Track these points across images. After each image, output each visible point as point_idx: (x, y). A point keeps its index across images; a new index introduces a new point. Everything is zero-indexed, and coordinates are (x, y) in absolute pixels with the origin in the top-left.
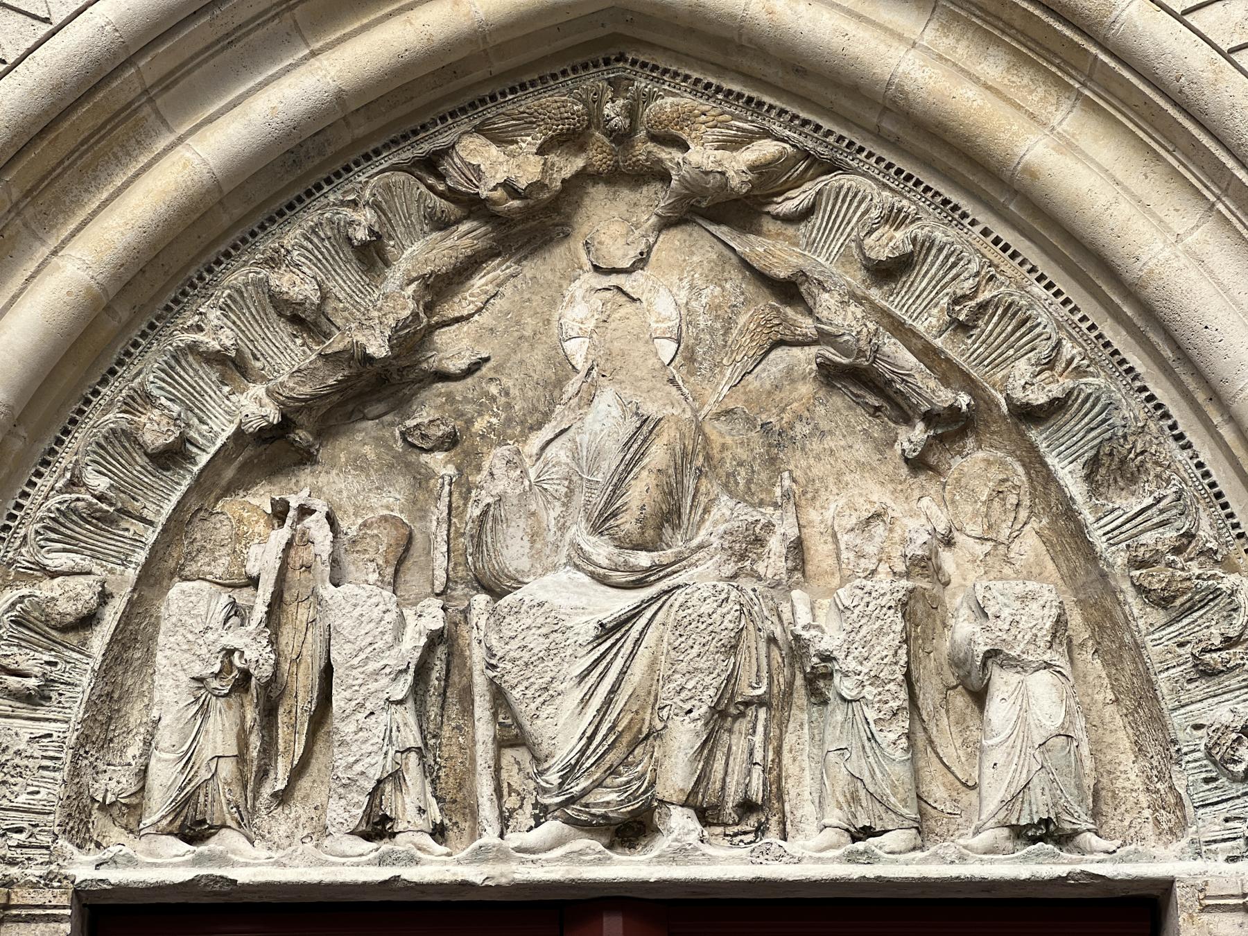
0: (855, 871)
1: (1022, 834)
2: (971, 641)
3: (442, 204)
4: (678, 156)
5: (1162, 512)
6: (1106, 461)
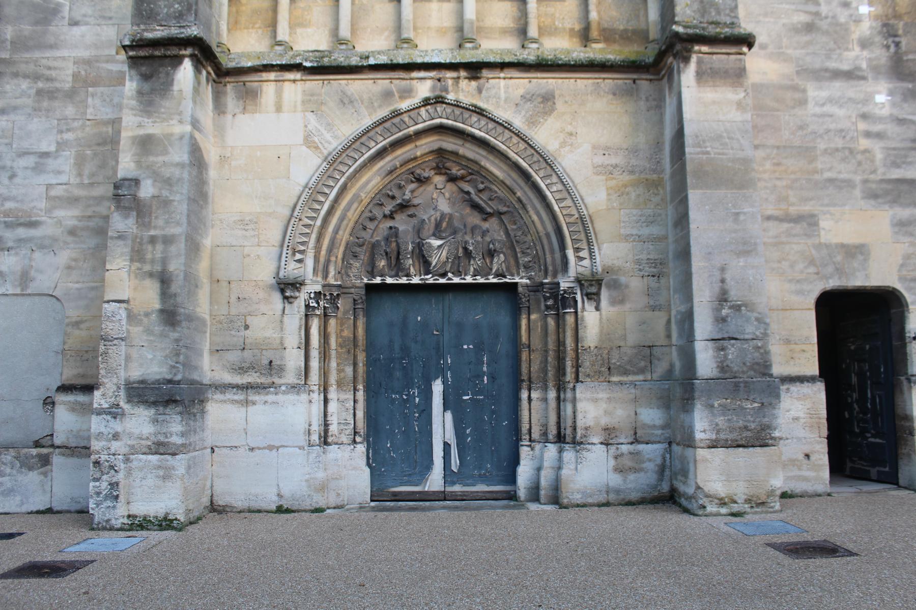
1: (499, 275)
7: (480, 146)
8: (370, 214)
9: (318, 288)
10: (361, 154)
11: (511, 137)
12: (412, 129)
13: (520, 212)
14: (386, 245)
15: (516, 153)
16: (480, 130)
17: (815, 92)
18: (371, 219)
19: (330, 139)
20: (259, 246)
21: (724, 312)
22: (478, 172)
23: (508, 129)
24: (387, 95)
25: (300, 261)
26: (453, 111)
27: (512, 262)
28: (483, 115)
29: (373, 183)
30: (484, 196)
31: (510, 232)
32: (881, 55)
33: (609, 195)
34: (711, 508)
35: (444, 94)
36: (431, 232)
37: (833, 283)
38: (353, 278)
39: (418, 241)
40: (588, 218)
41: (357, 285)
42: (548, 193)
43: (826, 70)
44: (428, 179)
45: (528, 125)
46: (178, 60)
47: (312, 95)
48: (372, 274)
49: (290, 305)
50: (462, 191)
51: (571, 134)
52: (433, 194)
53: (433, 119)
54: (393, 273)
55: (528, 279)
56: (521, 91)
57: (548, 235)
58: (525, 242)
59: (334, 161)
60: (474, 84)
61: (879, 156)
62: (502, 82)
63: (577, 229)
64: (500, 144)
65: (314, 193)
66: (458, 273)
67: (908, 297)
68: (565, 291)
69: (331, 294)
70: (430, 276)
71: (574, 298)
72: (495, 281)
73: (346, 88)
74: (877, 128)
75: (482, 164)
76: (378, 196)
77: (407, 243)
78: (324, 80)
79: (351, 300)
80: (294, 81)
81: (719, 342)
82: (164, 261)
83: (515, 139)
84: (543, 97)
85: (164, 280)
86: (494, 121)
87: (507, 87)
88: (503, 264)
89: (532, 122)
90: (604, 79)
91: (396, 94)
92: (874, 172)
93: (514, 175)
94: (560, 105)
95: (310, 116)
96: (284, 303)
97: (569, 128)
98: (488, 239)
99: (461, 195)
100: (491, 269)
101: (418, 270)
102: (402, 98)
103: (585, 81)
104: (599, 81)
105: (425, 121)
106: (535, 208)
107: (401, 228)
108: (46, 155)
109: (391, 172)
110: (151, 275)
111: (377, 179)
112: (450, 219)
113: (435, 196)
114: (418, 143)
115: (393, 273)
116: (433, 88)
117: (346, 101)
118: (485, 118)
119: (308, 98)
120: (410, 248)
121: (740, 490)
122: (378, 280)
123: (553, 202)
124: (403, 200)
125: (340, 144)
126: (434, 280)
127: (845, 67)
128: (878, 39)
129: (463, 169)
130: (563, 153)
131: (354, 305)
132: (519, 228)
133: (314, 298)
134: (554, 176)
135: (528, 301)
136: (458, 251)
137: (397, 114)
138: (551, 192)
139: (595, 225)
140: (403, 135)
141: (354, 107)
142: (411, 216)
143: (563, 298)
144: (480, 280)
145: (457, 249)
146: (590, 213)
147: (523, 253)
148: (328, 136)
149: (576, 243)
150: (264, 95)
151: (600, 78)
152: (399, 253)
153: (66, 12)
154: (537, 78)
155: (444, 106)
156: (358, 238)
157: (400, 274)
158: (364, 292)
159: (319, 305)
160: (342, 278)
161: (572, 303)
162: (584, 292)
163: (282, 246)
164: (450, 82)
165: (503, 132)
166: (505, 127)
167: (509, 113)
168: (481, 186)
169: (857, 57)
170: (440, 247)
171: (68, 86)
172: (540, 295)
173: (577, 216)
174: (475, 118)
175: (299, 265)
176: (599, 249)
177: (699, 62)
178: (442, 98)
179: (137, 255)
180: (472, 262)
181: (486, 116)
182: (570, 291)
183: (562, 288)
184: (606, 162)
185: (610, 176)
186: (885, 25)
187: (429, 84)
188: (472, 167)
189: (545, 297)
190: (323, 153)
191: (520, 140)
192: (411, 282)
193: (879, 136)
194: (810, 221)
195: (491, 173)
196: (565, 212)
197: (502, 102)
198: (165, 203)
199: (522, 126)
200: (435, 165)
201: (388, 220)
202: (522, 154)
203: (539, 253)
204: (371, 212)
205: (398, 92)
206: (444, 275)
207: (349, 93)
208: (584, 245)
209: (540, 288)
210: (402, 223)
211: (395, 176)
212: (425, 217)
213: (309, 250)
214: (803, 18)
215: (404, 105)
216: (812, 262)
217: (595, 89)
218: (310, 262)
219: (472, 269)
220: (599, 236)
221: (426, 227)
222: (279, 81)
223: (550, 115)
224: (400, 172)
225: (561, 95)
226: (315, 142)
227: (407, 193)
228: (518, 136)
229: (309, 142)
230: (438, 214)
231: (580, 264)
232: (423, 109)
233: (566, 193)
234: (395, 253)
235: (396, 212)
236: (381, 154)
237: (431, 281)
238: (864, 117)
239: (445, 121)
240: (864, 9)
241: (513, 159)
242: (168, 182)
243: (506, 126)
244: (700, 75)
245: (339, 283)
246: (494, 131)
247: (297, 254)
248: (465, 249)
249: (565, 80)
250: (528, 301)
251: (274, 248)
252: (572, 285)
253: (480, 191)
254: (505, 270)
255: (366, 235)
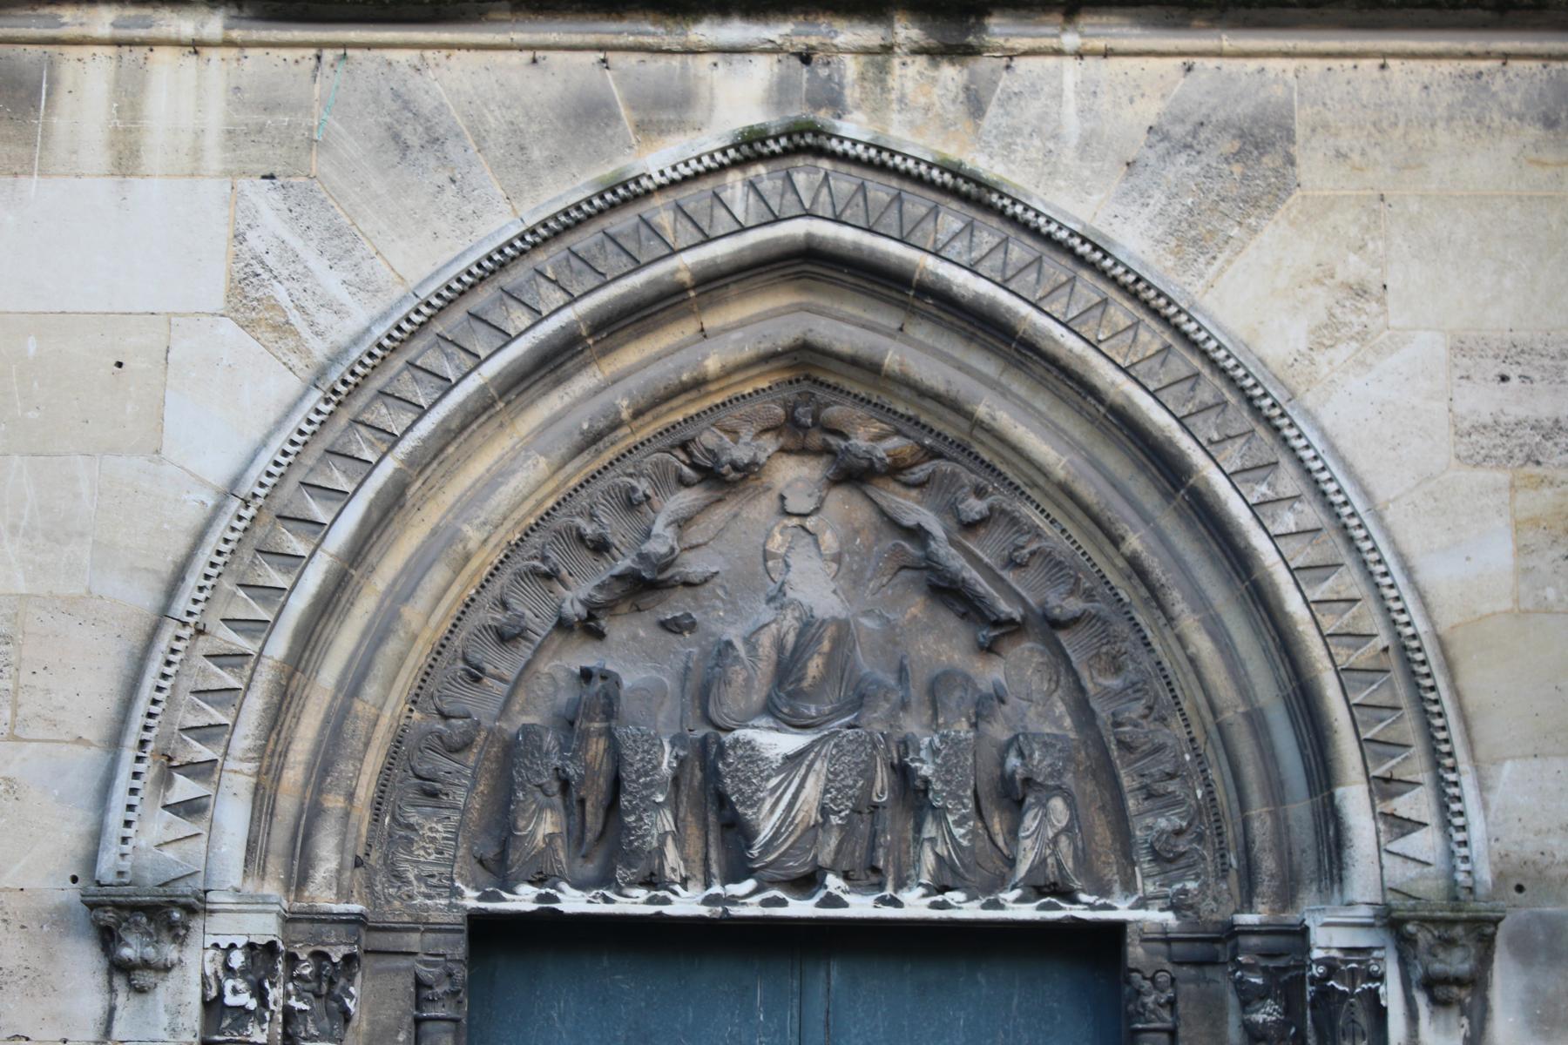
0: (936, 914)
1: (1038, 889)
2: (1014, 772)
3: (686, 470)
4: (843, 444)
5: (1135, 692)
6: (1104, 657)
7: (970, 339)
8: (500, 616)
9: (264, 928)
10: (469, 362)
11: (1105, 302)
12: (689, 259)
13: (1139, 618)
14: (563, 748)
15: (1125, 371)
16: (972, 269)
18: (506, 637)
19: (342, 294)
20: (17, 739)
22: (964, 448)
23: (1092, 266)
25: (191, 809)
26: (862, 188)
27: (1102, 833)
28: (989, 208)
29: (518, 482)
30: (988, 548)
31: (1095, 705)
33: (1522, 550)
35: (823, 117)
36: (757, 698)
38: (418, 888)
39: (699, 733)
40: (1431, 652)
41: (435, 917)
42: (1259, 541)
44: (749, 471)
45: (1177, 252)
47: (269, 108)
48: (500, 874)
49: (136, 1000)
50: (892, 523)
51: (1360, 291)
52: (769, 535)
53: (777, 220)
54: (590, 869)
55: (1173, 907)
56: (1150, 110)
57: (1256, 720)
58: (1159, 749)
60: (951, 74)
62: (1069, 63)
63: (1383, 698)
64: (1058, 331)
66: (867, 876)
68: (1331, 966)
69: (320, 957)
70: (749, 884)
71: (1374, 996)
72: (1028, 912)
73: (416, 81)
75: (982, 411)
76: (536, 539)
77: (654, 742)
78: (321, 45)
79: (405, 984)
80: (196, 46)
83: (1122, 311)
84: (1241, 135)
86: (1035, 233)
87: (1090, 91)
88: (1064, 842)
90: (1506, 57)
91: (623, 112)
93: (1116, 462)
94: (1313, 169)
95: (261, 197)
96: (112, 990)
97: (1354, 267)
98: (999, 731)
99: (889, 542)
100: (1012, 863)
101: (698, 859)
102: (648, 128)
103: (1424, 68)
104: (1483, 65)
105: (743, 229)
106: (1200, 602)
107: (632, 677)
109: (592, 440)
111: (535, 468)
112: (837, 642)
113: (777, 543)
114: (712, 320)
115: (590, 869)
116: (781, 92)
118: (994, 222)
119: (257, 118)
120: (667, 763)
122: (524, 899)
123: (1282, 578)
124: (643, 557)
125: (385, 316)
126: (766, 903)
129: (898, 432)
130: (1325, 370)
131: (418, 1007)
132: (1135, 689)
133: (243, 973)
134: (1287, 469)
135: (1172, 1003)
136: (871, 782)
138: (1272, 538)
139: (1464, 682)
140: (651, 283)
141: (444, 161)
142: (673, 627)
143: (1325, 994)
145: (868, 774)
146: (1442, 628)
147: (1150, 795)
148: (332, 282)
149: (1381, 758)
150: (64, 100)
151: (1487, 55)
152: (616, 785)
154: (1219, 54)
155: (825, 164)
156: (445, 716)
157: (620, 872)
158: (460, 951)
159: (263, 1002)
160: (370, 886)
161: (1363, 1020)
162: (1417, 973)
163: (115, 742)
164: (851, 67)
165: (1072, 280)
166: (1081, 260)
167: (1096, 198)
168: (975, 507)
170: (793, 760)
172: (1221, 980)
173: (1383, 640)
174: (952, 219)
175: (184, 827)
176: (1483, 787)
178: (817, 132)
180: (930, 830)
181: (1001, 213)
182: (1357, 963)
183: (1317, 954)
184: (1515, 412)
185: (1531, 469)
187: (762, 70)
188: (938, 426)
189: (1240, 986)
190: (309, 353)
191: (1140, 314)
192: (667, 910)
195: (1016, 449)
196: (1330, 624)
197: (1069, 156)
199: (1150, 258)
200: (780, 411)
201: (576, 639)
202: (1150, 373)
203: (1220, 795)
204: (505, 605)
205: (633, 107)
206: (807, 883)
207: (427, 104)
208: (1416, 766)
209: (1223, 952)
211: (609, 455)
212: (734, 634)
213: (231, 764)
217: (1466, 101)
219: (929, 860)
220: (1480, 728)
221: (738, 675)
222: (131, 43)
223: (1272, 210)
224: (631, 441)
225: (1320, 127)
226: (275, 306)
227: (658, 528)
228: (1134, 296)
230: (790, 623)
231: (1398, 846)
232: (734, 178)
233: (1339, 541)
234: (602, 783)
235: (609, 607)
237: (752, 909)
239: (826, 230)
241: (1113, 396)
245: (356, 907)
246: (1031, 276)
247: (180, 779)
248: (902, 773)
249: (1334, 63)
250: (1172, 1003)
251: (80, 749)
252: (1361, 939)
253: (970, 527)
254: (1069, 865)
255: (481, 704)
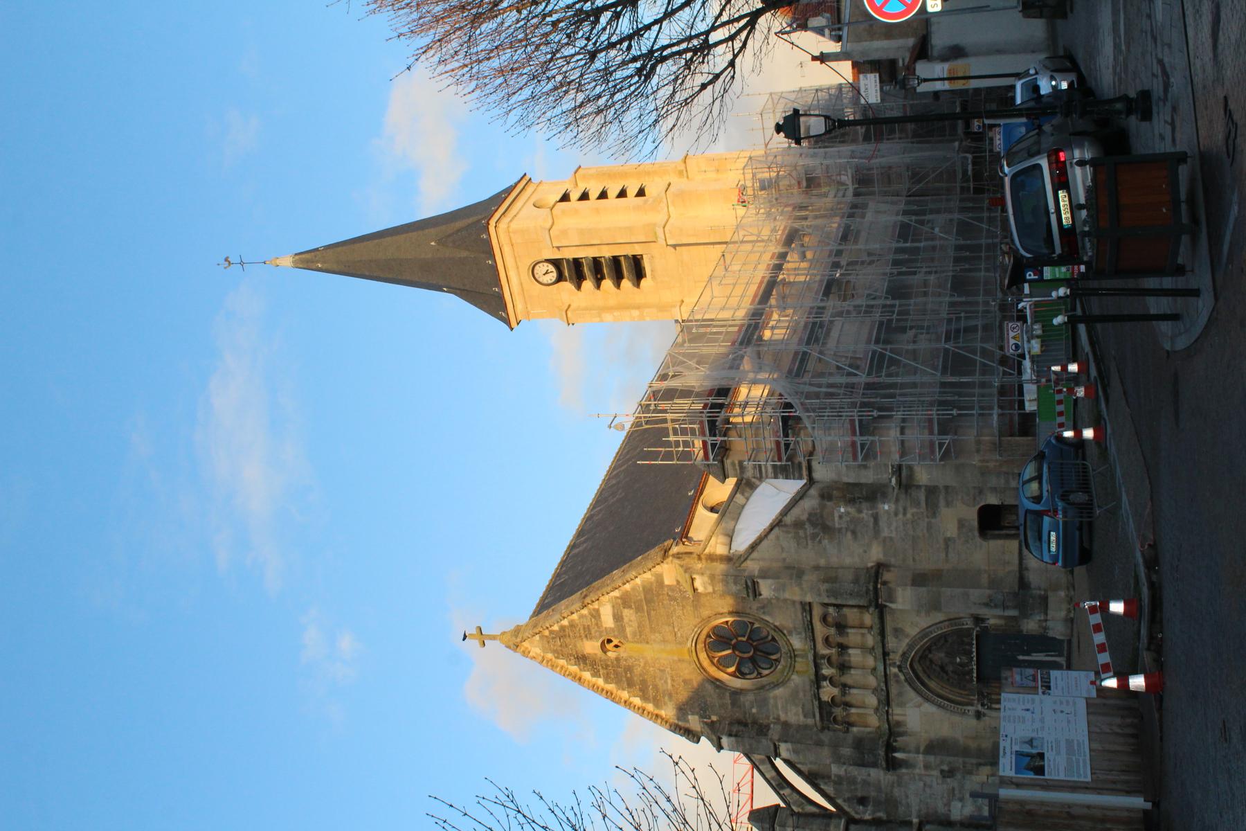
17: (885, 533)
21: (992, 605)
24: (898, 682)
32: (865, 505)
34: (1072, 615)
37: (976, 533)
43: (874, 528)
46: (895, 757)
48: (972, 681)
51: (912, 623)
56: (894, 639)
59: (927, 699)
61: (915, 510)
65: (939, 706)
67: (982, 504)
74: (901, 509)
81: (1005, 608)
82: (972, 764)
85: (979, 765)
89: (907, 636)
92: (923, 513)
94: (900, 626)
108: (925, 785)
110: (978, 769)
116: (894, 667)
117: (900, 694)
121: (1065, 606)
127: (872, 520)
128: (857, 506)
137: (906, 680)
144: (974, 646)
153: (864, 777)
169: (866, 514)
171: (896, 778)
177: (885, 601)
179: (970, 773)
186: (849, 501)
193: (905, 509)
194: (947, 541)
198: (950, 763)
210: (950, 668)
214: (849, 535)
215: (902, 678)
216: (967, 541)
218: (970, 708)
229: (919, 706)
236: (923, 684)
238: (896, 514)
239: (908, 663)
240: (842, 510)
242: (942, 763)
243: (911, 647)
244: (892, 602)
